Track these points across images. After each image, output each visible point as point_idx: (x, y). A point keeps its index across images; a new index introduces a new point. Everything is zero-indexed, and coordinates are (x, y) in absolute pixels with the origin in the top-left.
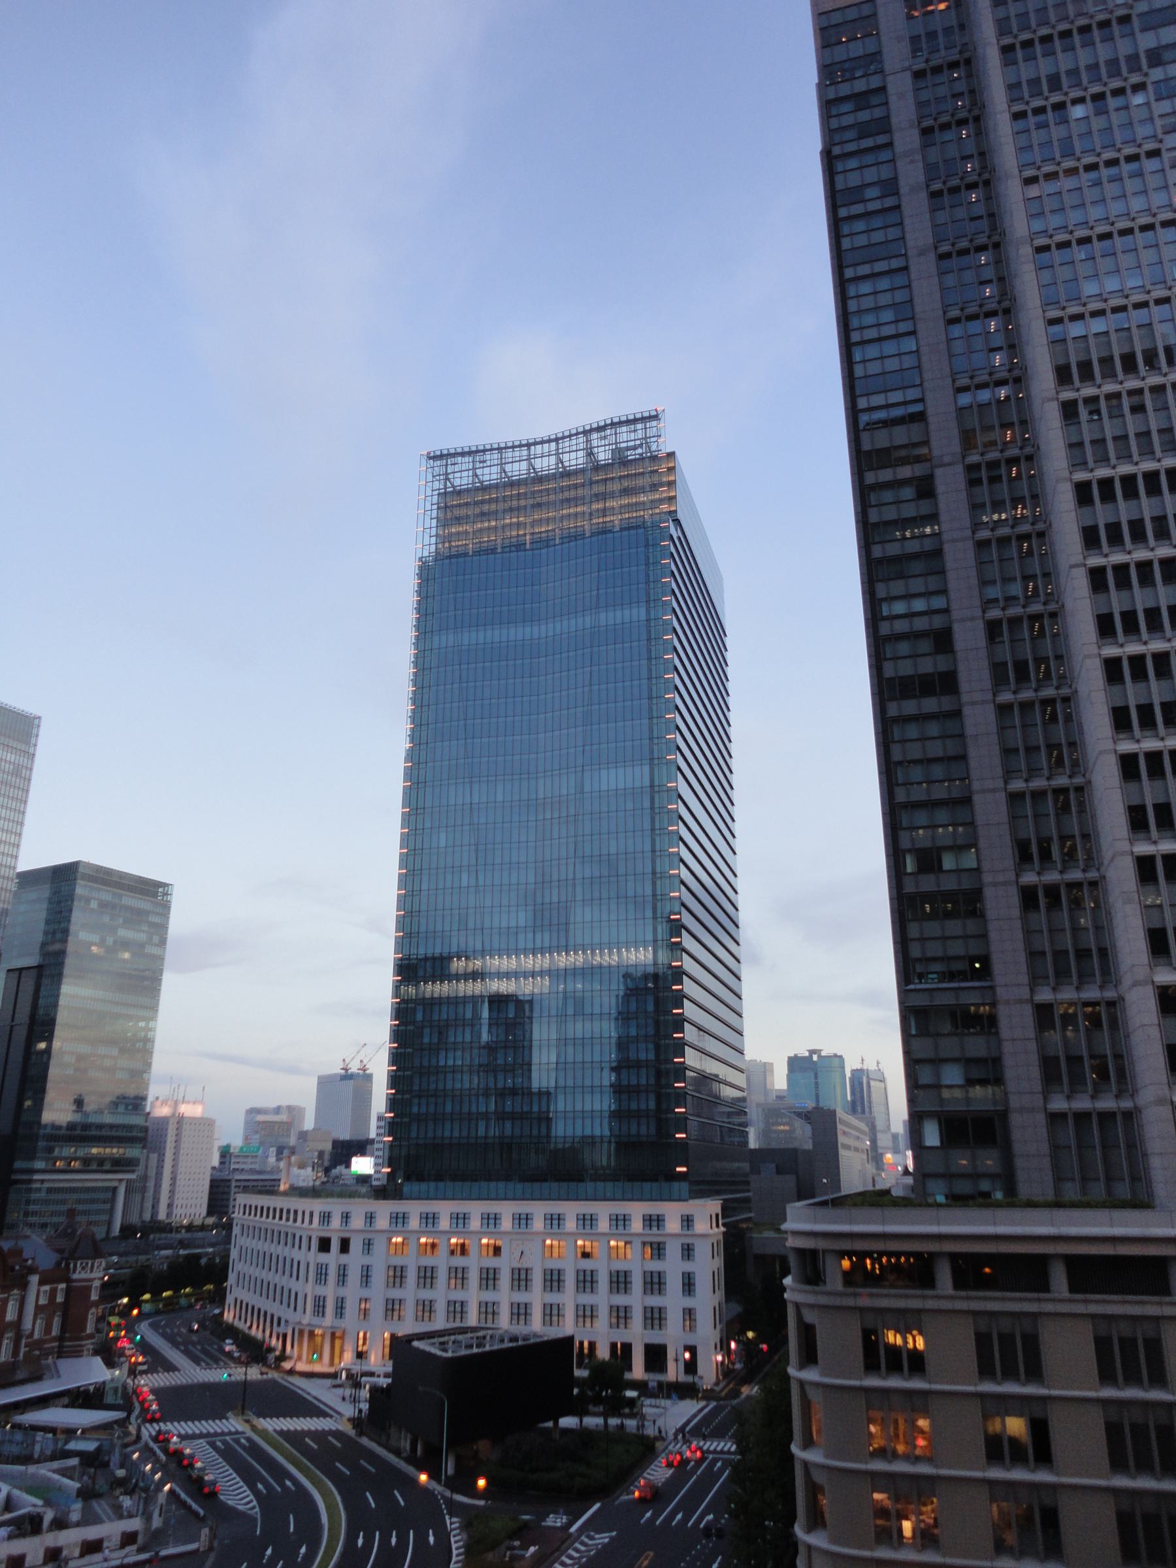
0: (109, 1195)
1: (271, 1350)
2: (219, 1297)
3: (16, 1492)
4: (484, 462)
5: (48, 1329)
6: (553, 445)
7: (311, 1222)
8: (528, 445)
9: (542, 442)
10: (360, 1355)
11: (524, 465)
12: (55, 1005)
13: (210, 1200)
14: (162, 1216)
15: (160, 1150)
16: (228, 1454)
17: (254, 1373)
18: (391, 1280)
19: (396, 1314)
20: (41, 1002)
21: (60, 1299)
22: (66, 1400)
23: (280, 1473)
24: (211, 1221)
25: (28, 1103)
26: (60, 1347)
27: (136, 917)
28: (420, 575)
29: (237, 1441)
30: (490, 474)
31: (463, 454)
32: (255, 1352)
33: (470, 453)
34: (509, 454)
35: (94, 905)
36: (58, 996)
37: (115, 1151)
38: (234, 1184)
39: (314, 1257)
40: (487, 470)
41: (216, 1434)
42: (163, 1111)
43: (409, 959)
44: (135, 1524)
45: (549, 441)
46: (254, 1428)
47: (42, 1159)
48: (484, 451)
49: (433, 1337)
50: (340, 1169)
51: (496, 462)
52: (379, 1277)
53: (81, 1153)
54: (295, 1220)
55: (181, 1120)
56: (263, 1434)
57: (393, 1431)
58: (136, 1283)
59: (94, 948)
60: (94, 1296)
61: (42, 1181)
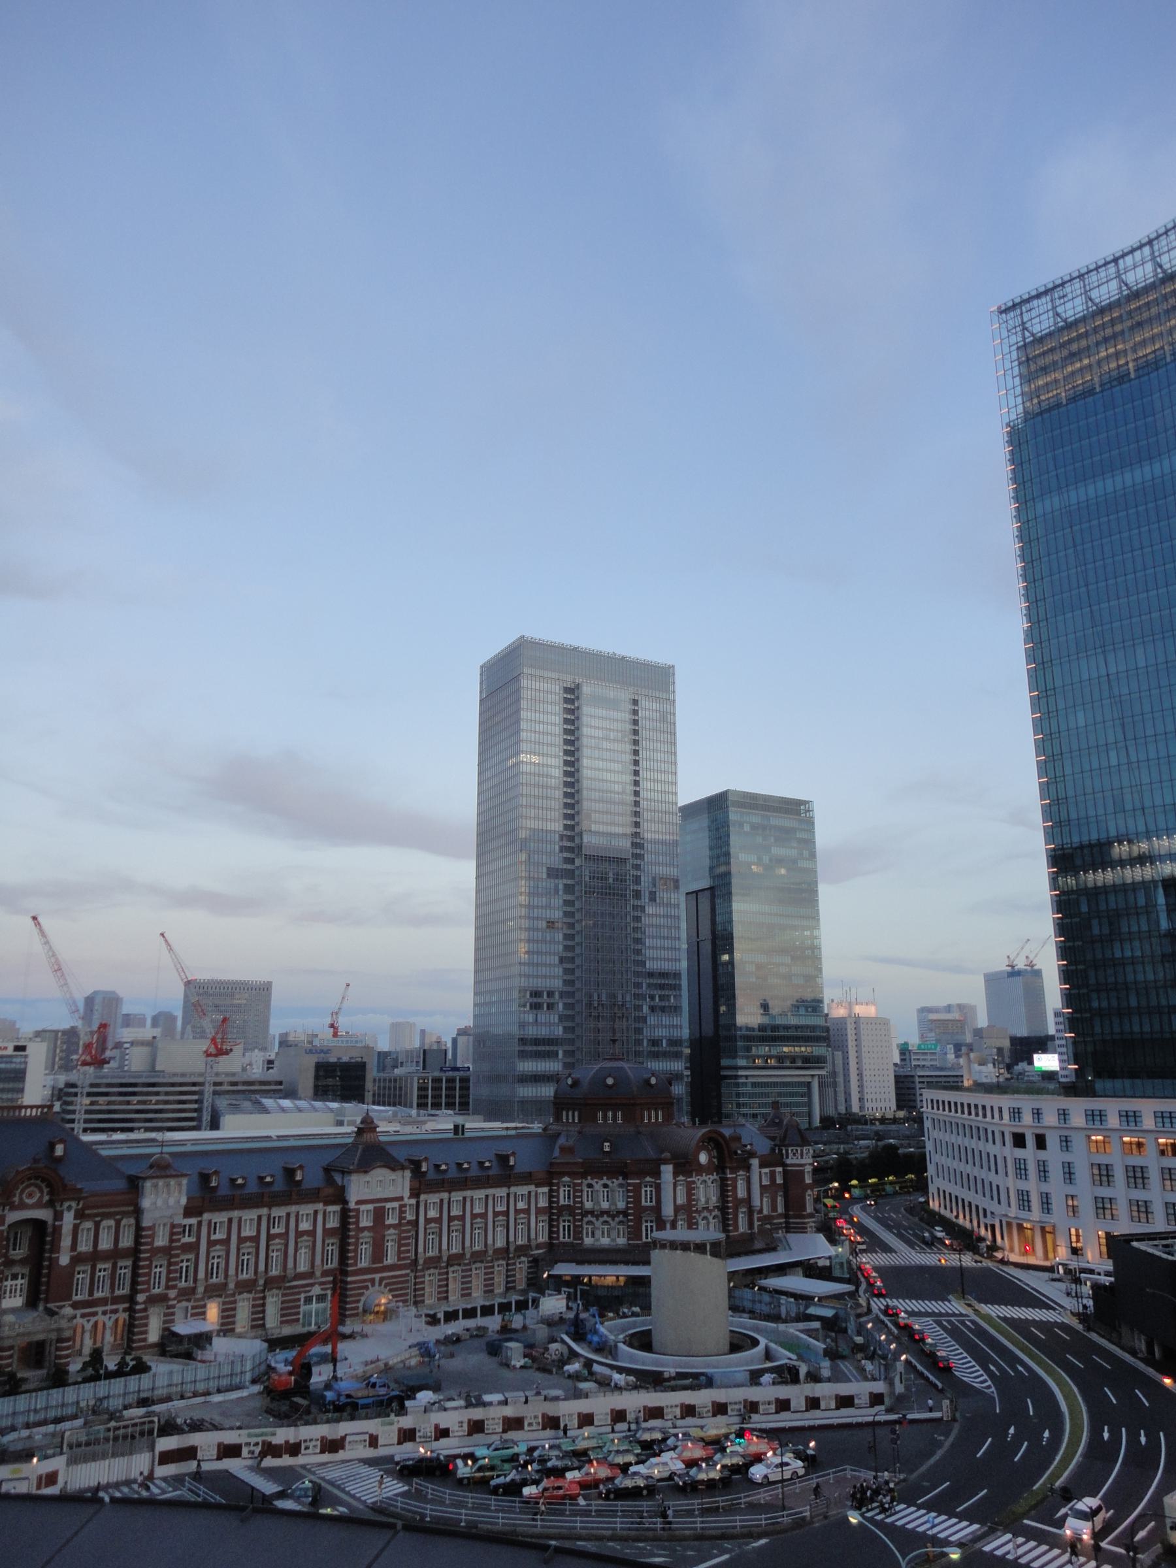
0: (805, 1090)
1: (983, 1239)
2: (922, 1186)
3: (772, 1345)
4: (1064, 296)
5: (774, 1208)
6: (1147, 250)
7: (1001, 1118)
8: (1115, 260)
9: (1132, 251)
10: (1075, 1251)
11: (1114, 285)
12: (730, 921)
14: (855, 1109)
15: (843, 1047)
16: (955, 1333)
17: (968, 1260)
18: (1097, 1178)
19: (1108, 1212)
20: (718, 919)
21: (779, 1181)
22: (800, 1270)
23: (1013, 1360)
24: (901, 1114)
25: (723, 1009)
26: (786, 1223)
27: (785, 835)
28: (1010, 442)
29: (963, 1323)
30: (1073, 308)
31: (1038, 296)
32: (967, 1241)
33: (1046, 292)
34: (1094, 277)
35: (747, 828)
36: (731, 913)
37: (802, 1050)
38: (917, 1080)
39: (1010, 1152)
40: (1069, 305)
41: (941, 1315)
42: (839, 1012)
43: (1063, 849)
44: (879, 1387)
45: (1141, 247)
46: (975, 1310)
47: (743, 1057)
48: (1063, 284)
49: (1155, 1239)
50: (1022, 1066)
51: (1078, 292)
52: (1083, 1174)
53: (774, 1052)
54: (985, 1116)
55: (857, 1020)
56: (988, 1318)
57: (1125, 1330)
58: (844, 1170)
60: (808, 1180)
61: (747, 1077)
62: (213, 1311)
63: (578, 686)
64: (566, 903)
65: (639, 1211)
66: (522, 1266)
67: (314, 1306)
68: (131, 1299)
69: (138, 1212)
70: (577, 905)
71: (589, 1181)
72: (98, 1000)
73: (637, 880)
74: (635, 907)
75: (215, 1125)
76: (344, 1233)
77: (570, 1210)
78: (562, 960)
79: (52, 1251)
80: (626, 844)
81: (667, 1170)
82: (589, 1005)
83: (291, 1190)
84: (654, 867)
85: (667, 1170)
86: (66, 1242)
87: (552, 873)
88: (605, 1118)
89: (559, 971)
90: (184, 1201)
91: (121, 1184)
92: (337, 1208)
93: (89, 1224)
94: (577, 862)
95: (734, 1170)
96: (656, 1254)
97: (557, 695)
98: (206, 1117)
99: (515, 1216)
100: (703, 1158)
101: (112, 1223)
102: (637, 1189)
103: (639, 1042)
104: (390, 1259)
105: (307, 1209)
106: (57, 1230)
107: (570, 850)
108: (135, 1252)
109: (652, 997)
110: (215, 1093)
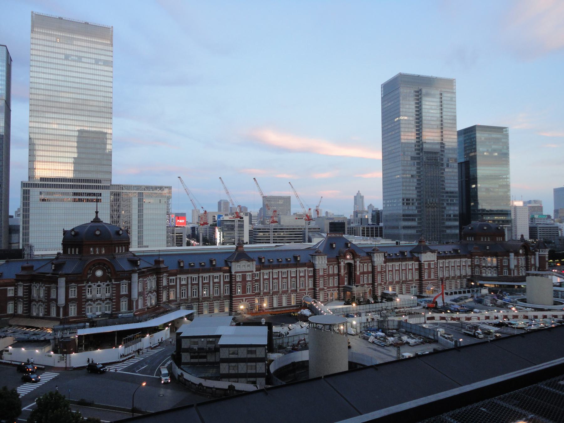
13: (530, 234)
14: (514, 238)
20: (471, 173)
25: (472, 204)
27: (497, 140)
38: (538, 228)
53: (492, 218)
55: (515, 207)
59: (485, 153)
60: (547, 259)
62: (390, 289)
63: (421, 90)
64: (418, 168)
65: (502, 267)
66: (465, 281)
67: (413, 289)
68: (373, 284)
69: (372, 262)
70: (422, 169)
71: (484, 257)
72: (222, 203)
73: (442, 159)
74: (442, 169)
75: (310, 241)
76: (420, 269)
77: (479, 266)
78: (416, 188)
79: (355, 271)
80: (438, 147)
81: (512, 255)
82: (426, 203)
83: (402, 257)
84: (448, 155)
85: (512, 255)
86: (358, 269)
87: (413, 158)
88: (484, 239)
89: (415, 192)
90: (384, 259)
91: (365, 254)
92: (417, 263)
93: (361, 265)
94: (421, 154)
95: (531, 255)
96: (527, 278)
97: (413, 93)
98: (307, 239)
99: (461, 266)
100: (521, 252)
101: (366, 264)
102: (501, 260)
103: (443, 216)
104: (432, 277)
105: (410, 263)
106: (355, 266)
107: (418, 150)
108: (373, 271)
109: (447, 200)
110: (309, 232)
